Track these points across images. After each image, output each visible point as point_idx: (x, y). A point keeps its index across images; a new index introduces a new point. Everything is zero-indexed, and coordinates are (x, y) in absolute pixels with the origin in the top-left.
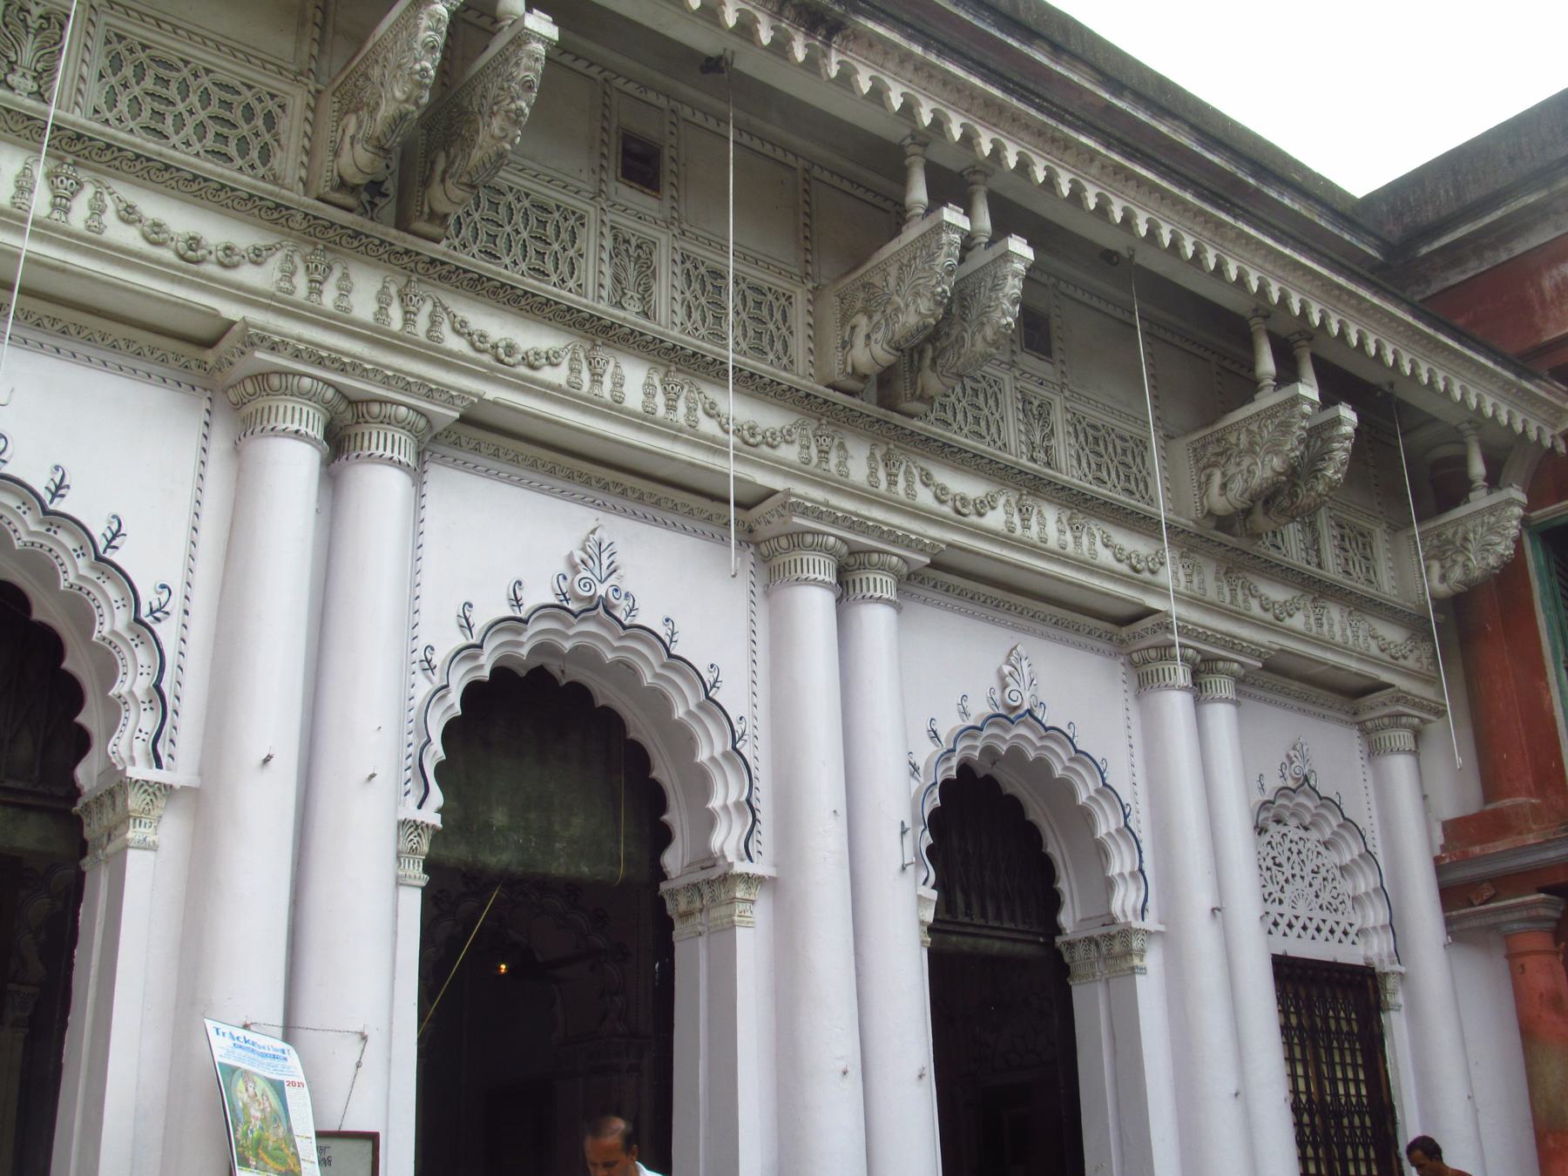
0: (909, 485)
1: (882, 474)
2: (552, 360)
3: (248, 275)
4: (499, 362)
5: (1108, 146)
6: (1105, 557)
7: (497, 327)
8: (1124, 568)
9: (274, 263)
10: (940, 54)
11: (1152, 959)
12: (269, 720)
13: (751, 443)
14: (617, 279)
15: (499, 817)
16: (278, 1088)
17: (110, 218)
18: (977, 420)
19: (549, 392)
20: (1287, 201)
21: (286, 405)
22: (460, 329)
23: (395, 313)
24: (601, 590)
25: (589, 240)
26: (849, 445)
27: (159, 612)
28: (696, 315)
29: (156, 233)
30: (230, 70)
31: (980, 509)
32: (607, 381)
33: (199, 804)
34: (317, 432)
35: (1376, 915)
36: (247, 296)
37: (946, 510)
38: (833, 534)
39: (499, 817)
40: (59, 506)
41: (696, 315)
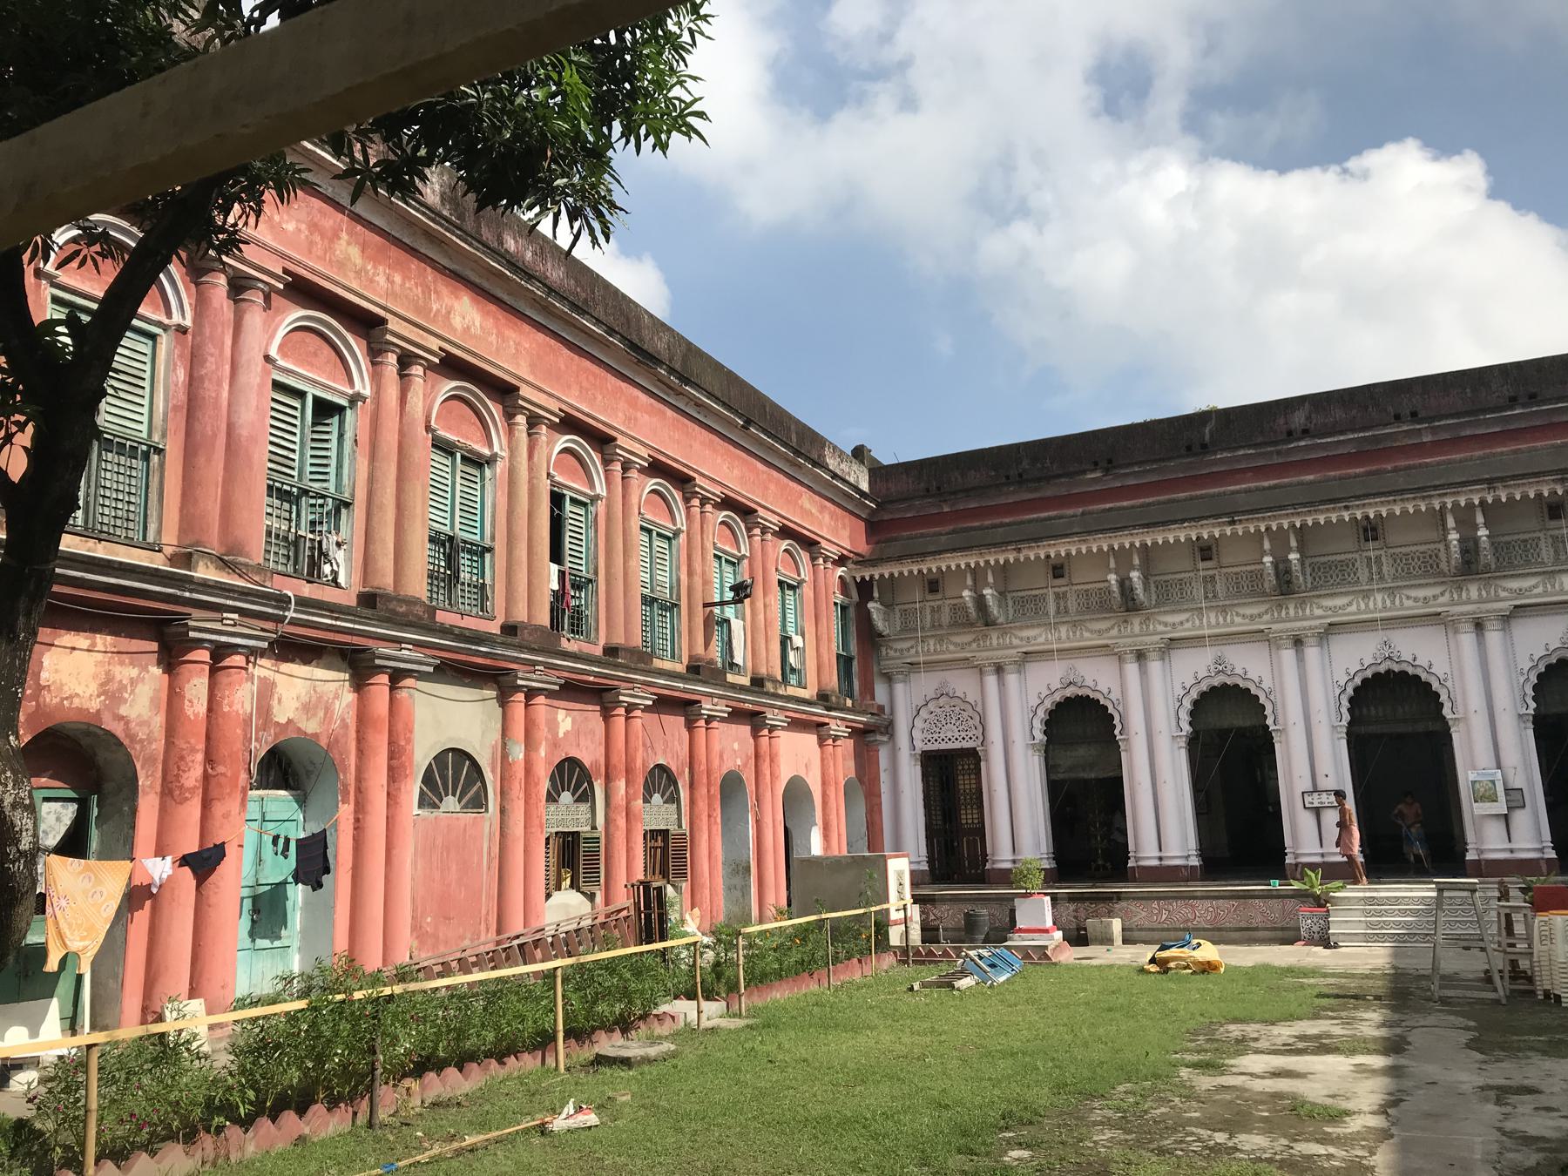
2: (1535, 587)
3: (1441, 600)
4: (1520, 593)
7: (1515, 584)
9: (1447, 595)
12: (1474, 700)
16: (1493, 782)
19: (1536, 596)
22: (1504, 590)
25: (1542, 544)
29: (1416, 600)
30: (1422, 548)
33: (1465, 719)
34: (1472, 628)
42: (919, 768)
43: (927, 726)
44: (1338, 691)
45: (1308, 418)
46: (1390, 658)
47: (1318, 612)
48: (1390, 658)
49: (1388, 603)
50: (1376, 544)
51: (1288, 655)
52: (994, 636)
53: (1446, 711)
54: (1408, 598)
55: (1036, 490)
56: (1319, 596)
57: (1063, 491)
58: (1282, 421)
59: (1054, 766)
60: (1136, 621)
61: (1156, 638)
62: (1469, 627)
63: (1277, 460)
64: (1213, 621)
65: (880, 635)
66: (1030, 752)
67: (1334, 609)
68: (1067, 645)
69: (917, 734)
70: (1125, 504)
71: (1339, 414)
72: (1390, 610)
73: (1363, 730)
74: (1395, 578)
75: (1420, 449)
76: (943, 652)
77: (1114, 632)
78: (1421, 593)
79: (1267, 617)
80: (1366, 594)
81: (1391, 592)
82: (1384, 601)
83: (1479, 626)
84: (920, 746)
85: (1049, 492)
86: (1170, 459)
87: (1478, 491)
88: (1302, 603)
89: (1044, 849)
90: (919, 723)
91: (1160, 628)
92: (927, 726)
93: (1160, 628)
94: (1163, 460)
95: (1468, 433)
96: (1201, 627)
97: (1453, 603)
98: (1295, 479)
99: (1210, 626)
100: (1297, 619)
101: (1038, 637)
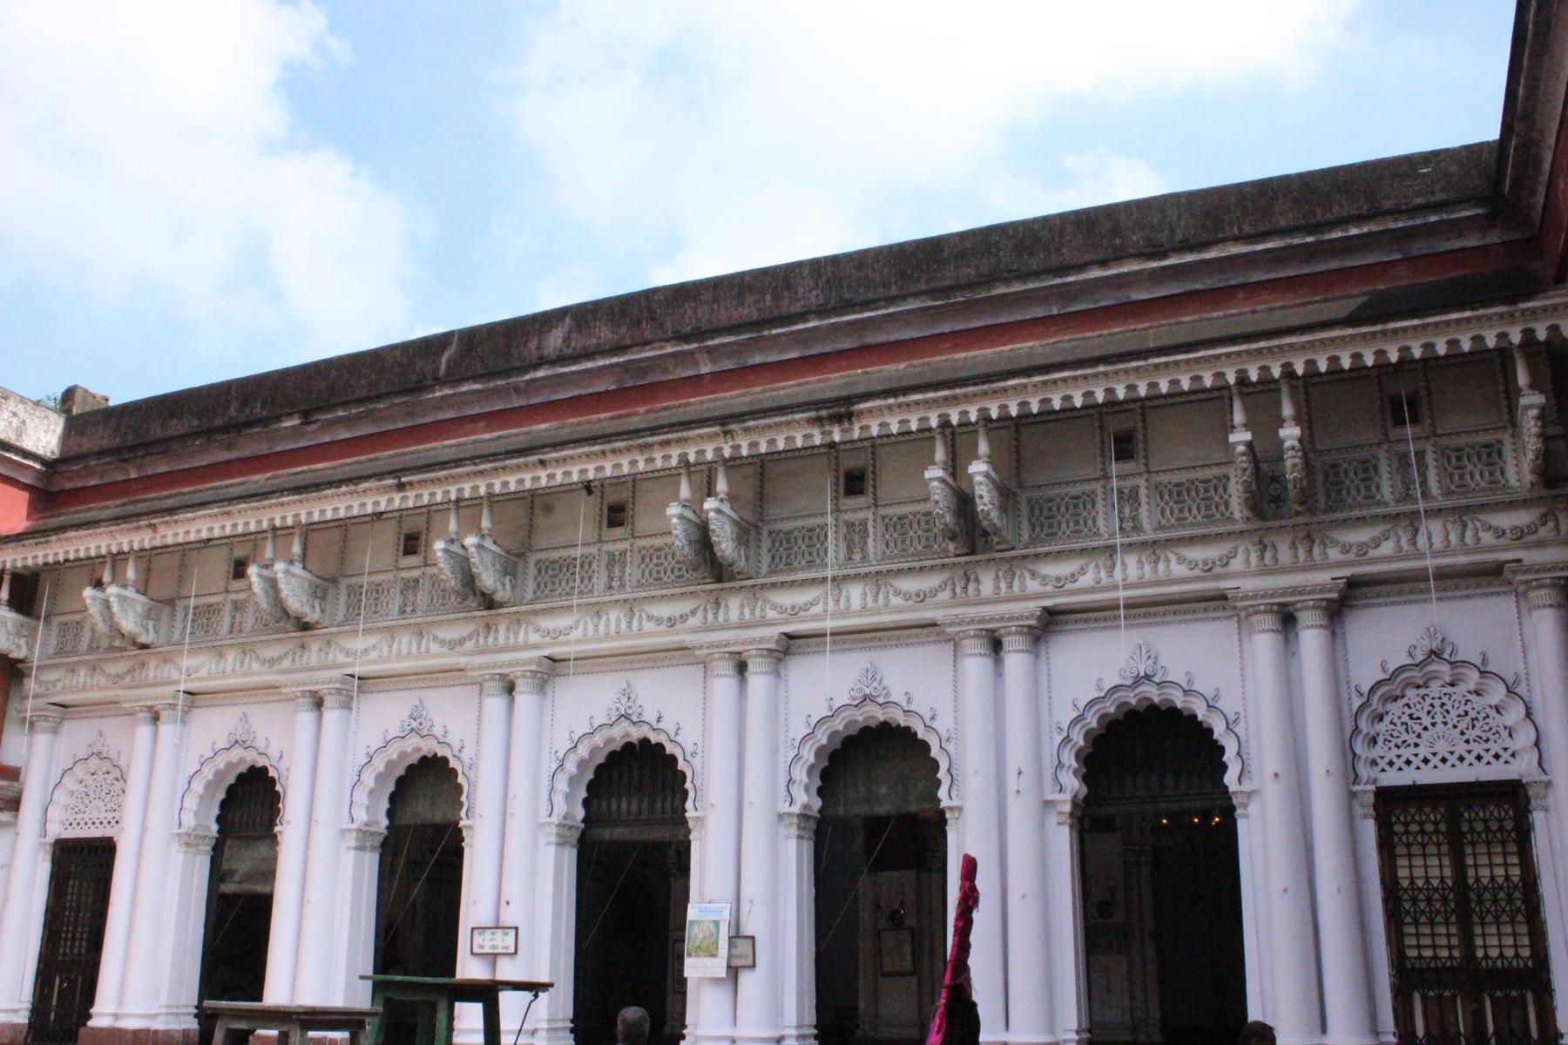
0: (1022, 584)
1: (1003, 585)
4: (795, 612)
5: (1029, 376)
6: (1179, 570)
8: (1196, 572)
9: (700, 614)
10: (904, 395)
11: (1254, 808)
13: (921, 598)
14: (848, 547)
15: (883, 791)
16: (717, 923)
17: (644, 622)
18: (1077, 523)
20: (1354, 231)
21: (715, 664)
22: (774, 607)
23: (747, 612)
24: (867, 691)
26: (981, 577)
27: (694, 754)
28: (892, 545)
29: (659, 621)
31: (1073, 578)
32: (842, 602)
35: (1525, 737)
36: (693, 631)
37: (1049, 588)
38: (971, 629)
39: (883, 791)
40: (661, 726)
41: (892, 545)
42: (44, 869)
43: (72, 801)
44: (555, 766)
45: (567, 339)
46: (626, 717)
47: (534, 638)
48: (626, 717)
49: (624, 624)
50: (618, 532)
51: (495, 704)
52: (153, 664)
53: (689, 805)
54: (650, 618)
55: (230, 446)
56: (536, 613)
57: (263, 448)
58: (533, 344)
59: (231, 873)
60: (315, 647)
61: (337, 673)
62: (726, 668)
63: (517, 402)
64: (404, 650)
65: (22, 661)
66: (175, 846)
67: (555, 635)
68: (232, 682)
69: (55, 814)
70: (320, 466)
71: (605, 333)
72: (626, 637)
73: (607, 834)
74: (640, 585)
75: (696, 384)
76: (92, 689)
77: (286, 663)
78: (665, 610)
79: (470, 645)
80: (597, 610)
81: (630, 606)
82: (618, 624)
83: (742, 668)
84: (57, 831)
85: (248, 449)
86: (379, 398)
87: (711, 437)
88: (517, 620)
89: (164, 999)
90: (61, 797)
91: (341, 658)
92: (72, 801)
93: (341, 658)
94: (370, 399)
95: (758, 359)
96: (387, 660)
97: (706, 629)
98: (524, 429)
99: (399, 657)
100: (507, 649)
101: (197, 668)
